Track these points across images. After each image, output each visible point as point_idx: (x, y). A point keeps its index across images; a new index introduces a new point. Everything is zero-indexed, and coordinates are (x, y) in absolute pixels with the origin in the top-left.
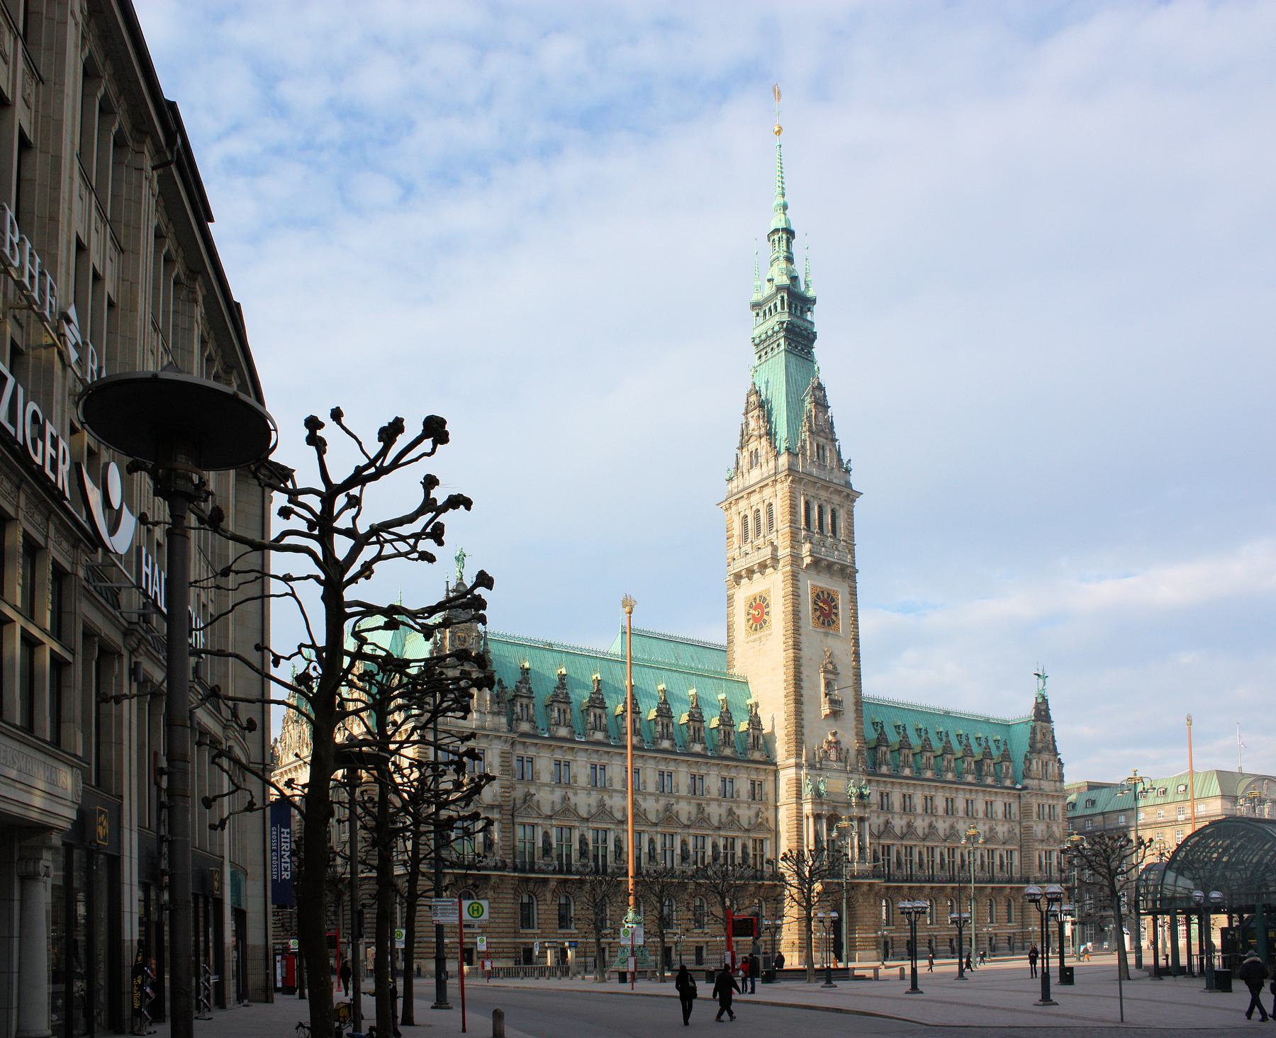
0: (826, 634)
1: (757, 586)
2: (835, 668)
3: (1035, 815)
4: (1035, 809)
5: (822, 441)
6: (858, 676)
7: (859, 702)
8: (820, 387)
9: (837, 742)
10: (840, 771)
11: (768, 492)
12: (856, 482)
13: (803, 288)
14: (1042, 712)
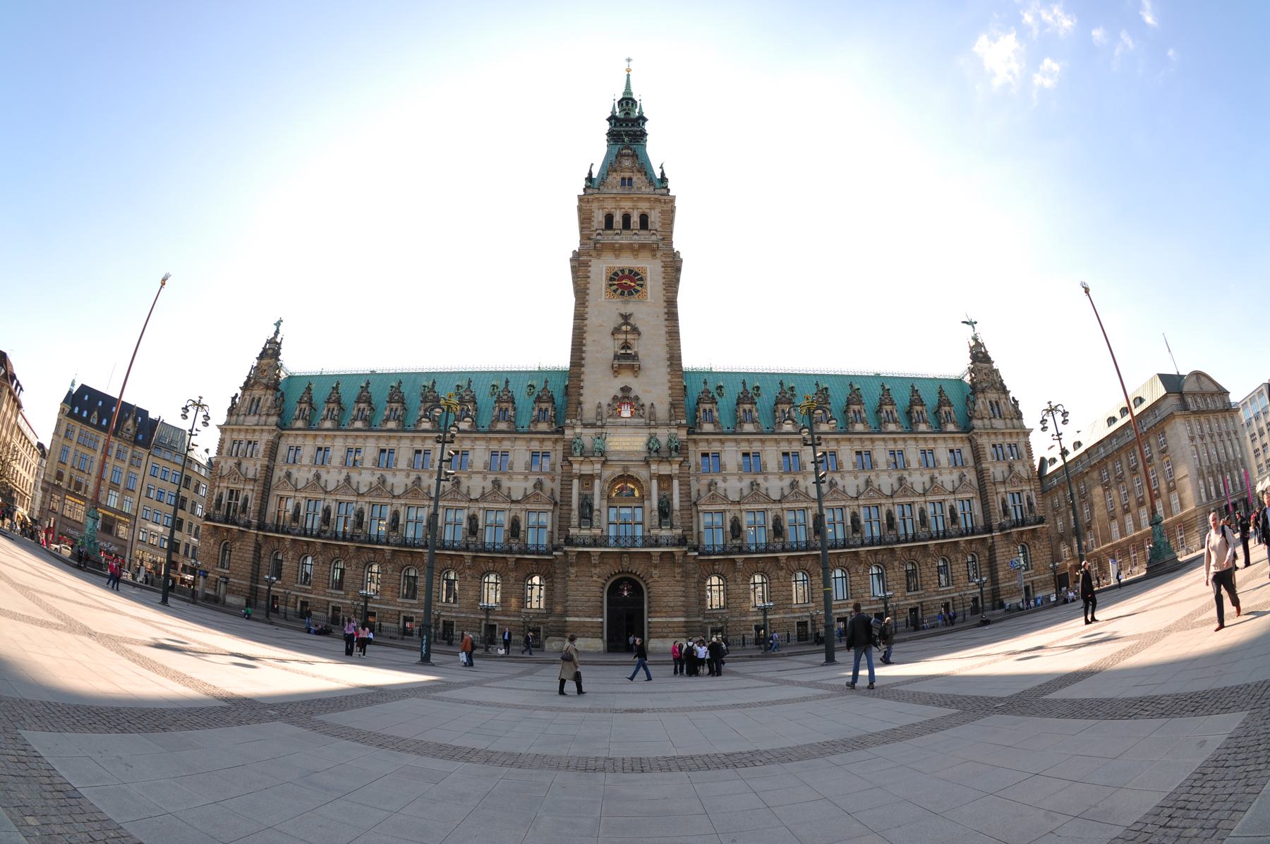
0: (626, 302)
3: (989, 457)
4: (989, 450)
6: (673, 335)
7: (674, 358)
9: (637, 398)
10: (636, 426)
14: (979, 356)
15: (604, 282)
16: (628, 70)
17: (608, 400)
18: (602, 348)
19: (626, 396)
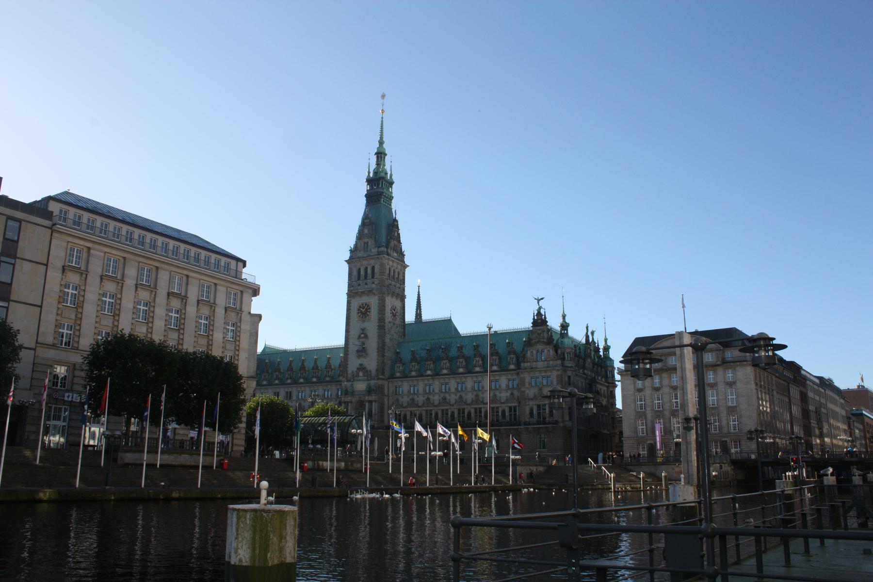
1: (364, 300)
8: (395, 221)
11: (372, 262)
12: (407, 260)
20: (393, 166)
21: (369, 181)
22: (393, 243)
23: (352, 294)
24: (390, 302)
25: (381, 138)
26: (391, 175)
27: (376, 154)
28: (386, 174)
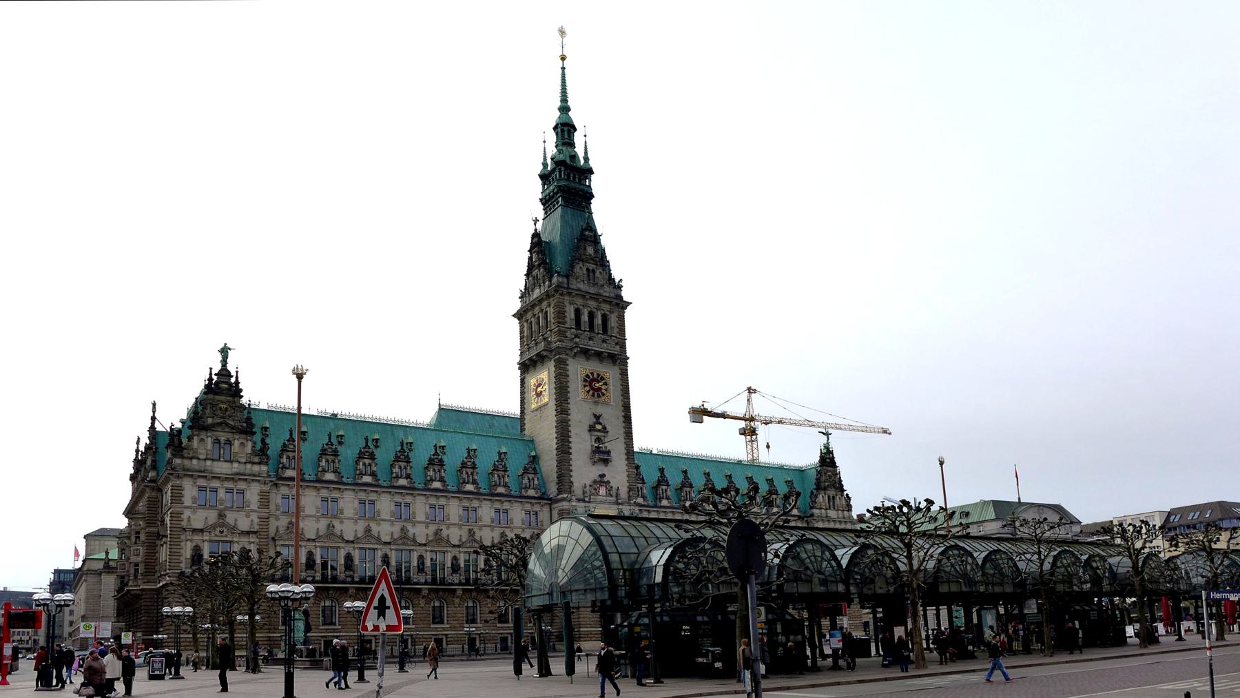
0: (596, 403)
2: (604, 428)
5: (591, 266)
7: (630, 453)
11: (545, 304)
13: (582, 162)
15: (580, 383)
16: (563, 68)
17: (588, 482)
18: (581, 444)
19: (601, 481)
20: (592, 143)
21: (544, 177)
22: (580, 269)
23: (527, 367)
24: (578, 369)
25: (564, 99)
26: (586, 159)
27: (555, 128)
28: (574, 157)
